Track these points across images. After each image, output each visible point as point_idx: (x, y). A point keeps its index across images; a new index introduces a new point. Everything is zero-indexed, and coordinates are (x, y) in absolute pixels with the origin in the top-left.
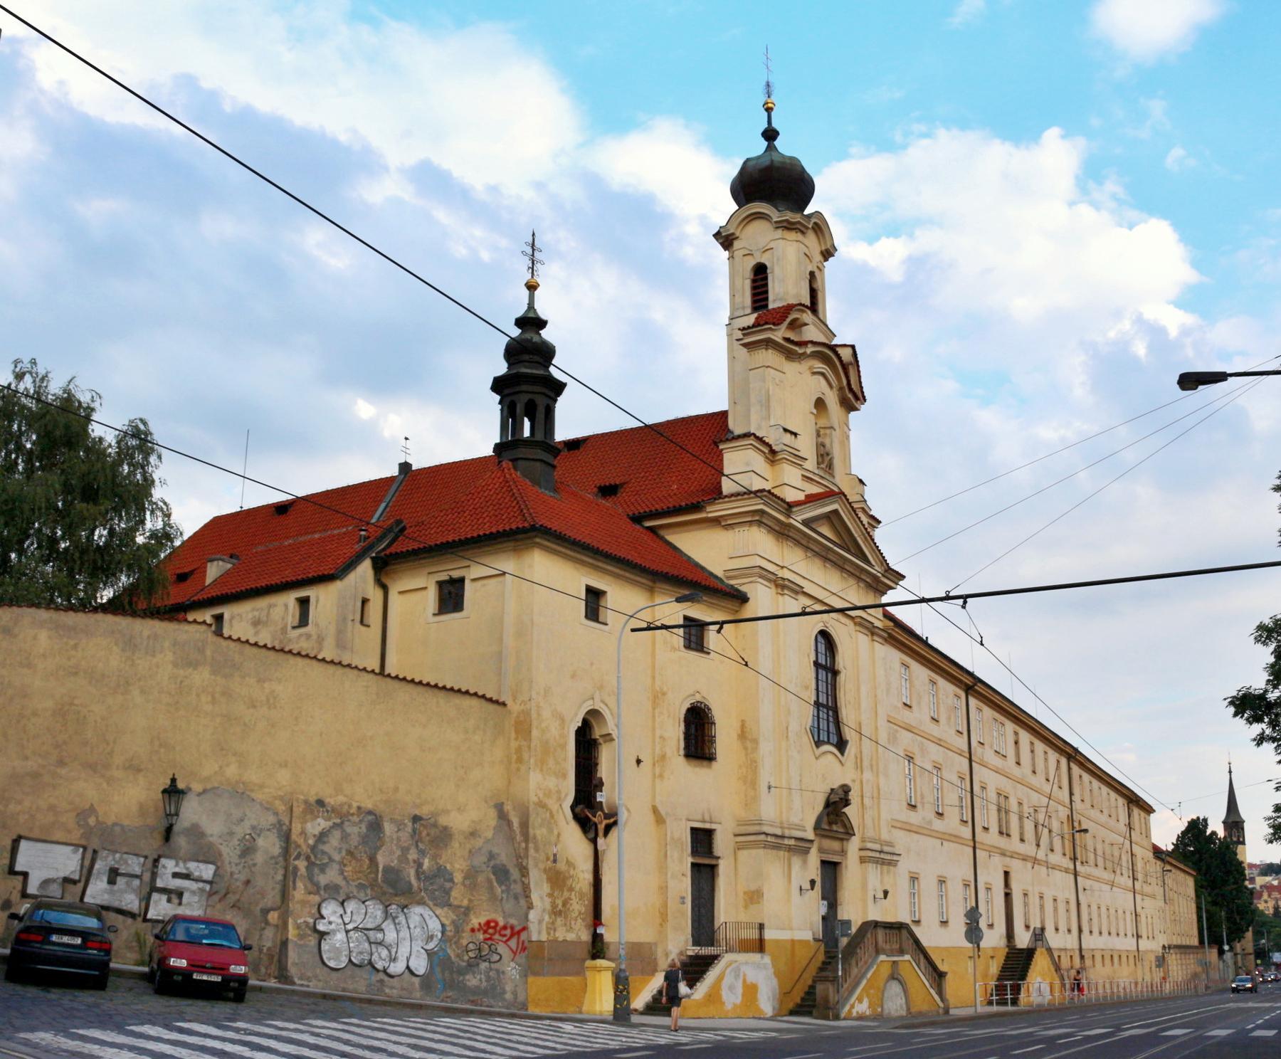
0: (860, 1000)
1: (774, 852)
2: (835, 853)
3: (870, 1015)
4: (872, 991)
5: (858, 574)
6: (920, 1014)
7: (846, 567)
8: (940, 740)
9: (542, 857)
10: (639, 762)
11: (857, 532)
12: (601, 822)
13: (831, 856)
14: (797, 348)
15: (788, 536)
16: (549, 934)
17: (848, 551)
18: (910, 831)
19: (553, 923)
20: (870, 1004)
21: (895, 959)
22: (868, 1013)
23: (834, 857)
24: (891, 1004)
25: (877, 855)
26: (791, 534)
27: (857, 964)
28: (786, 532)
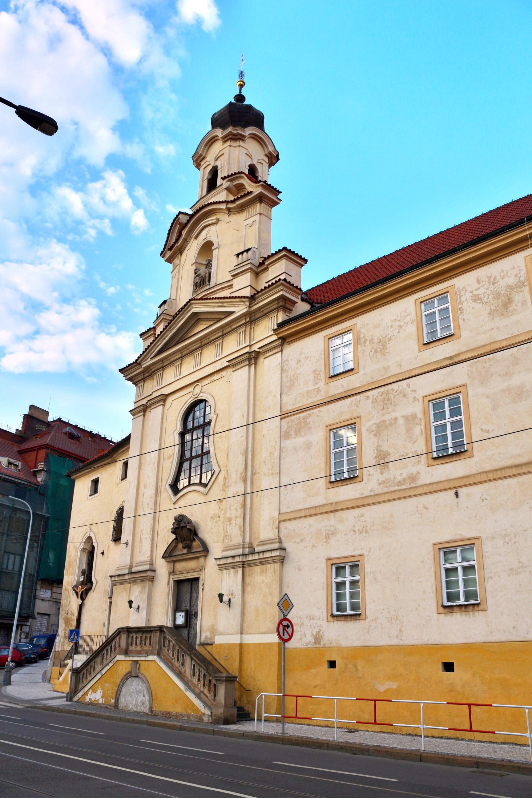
0: (93, 689)
1: (122, 586)
2: (193, 571)
3: (102, 704)
4: (107, 685)
5: (229, 329)
6: (167, 715)
7: (211, 339)
8: (451, 358)
9: (64, 612)
10: (103, 553)
11: (213, 307)
12: (80, 591)
13: (186, 575)
14: (176, 245)
15: (153, 372)
16: (62, 647)
17: (221, 320)
18: (334, 511)
19: (64, 642)
20: (104, 693)
21: (136, 659)
22: (101, 701)
23: (189, 574)
24: (129, 698)
25: (230, 560)
26: (153, 370)
27: (102, 662)
28: (151, 372)
